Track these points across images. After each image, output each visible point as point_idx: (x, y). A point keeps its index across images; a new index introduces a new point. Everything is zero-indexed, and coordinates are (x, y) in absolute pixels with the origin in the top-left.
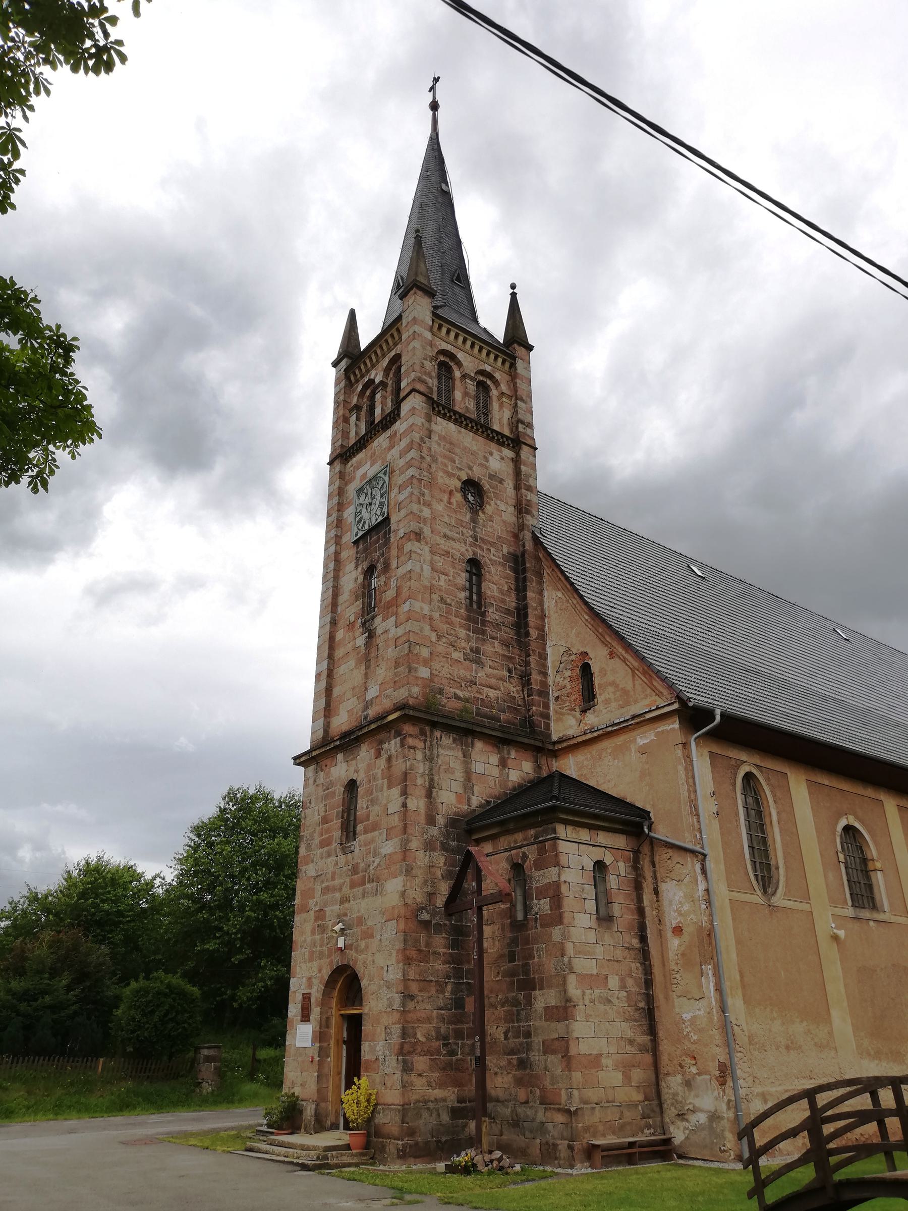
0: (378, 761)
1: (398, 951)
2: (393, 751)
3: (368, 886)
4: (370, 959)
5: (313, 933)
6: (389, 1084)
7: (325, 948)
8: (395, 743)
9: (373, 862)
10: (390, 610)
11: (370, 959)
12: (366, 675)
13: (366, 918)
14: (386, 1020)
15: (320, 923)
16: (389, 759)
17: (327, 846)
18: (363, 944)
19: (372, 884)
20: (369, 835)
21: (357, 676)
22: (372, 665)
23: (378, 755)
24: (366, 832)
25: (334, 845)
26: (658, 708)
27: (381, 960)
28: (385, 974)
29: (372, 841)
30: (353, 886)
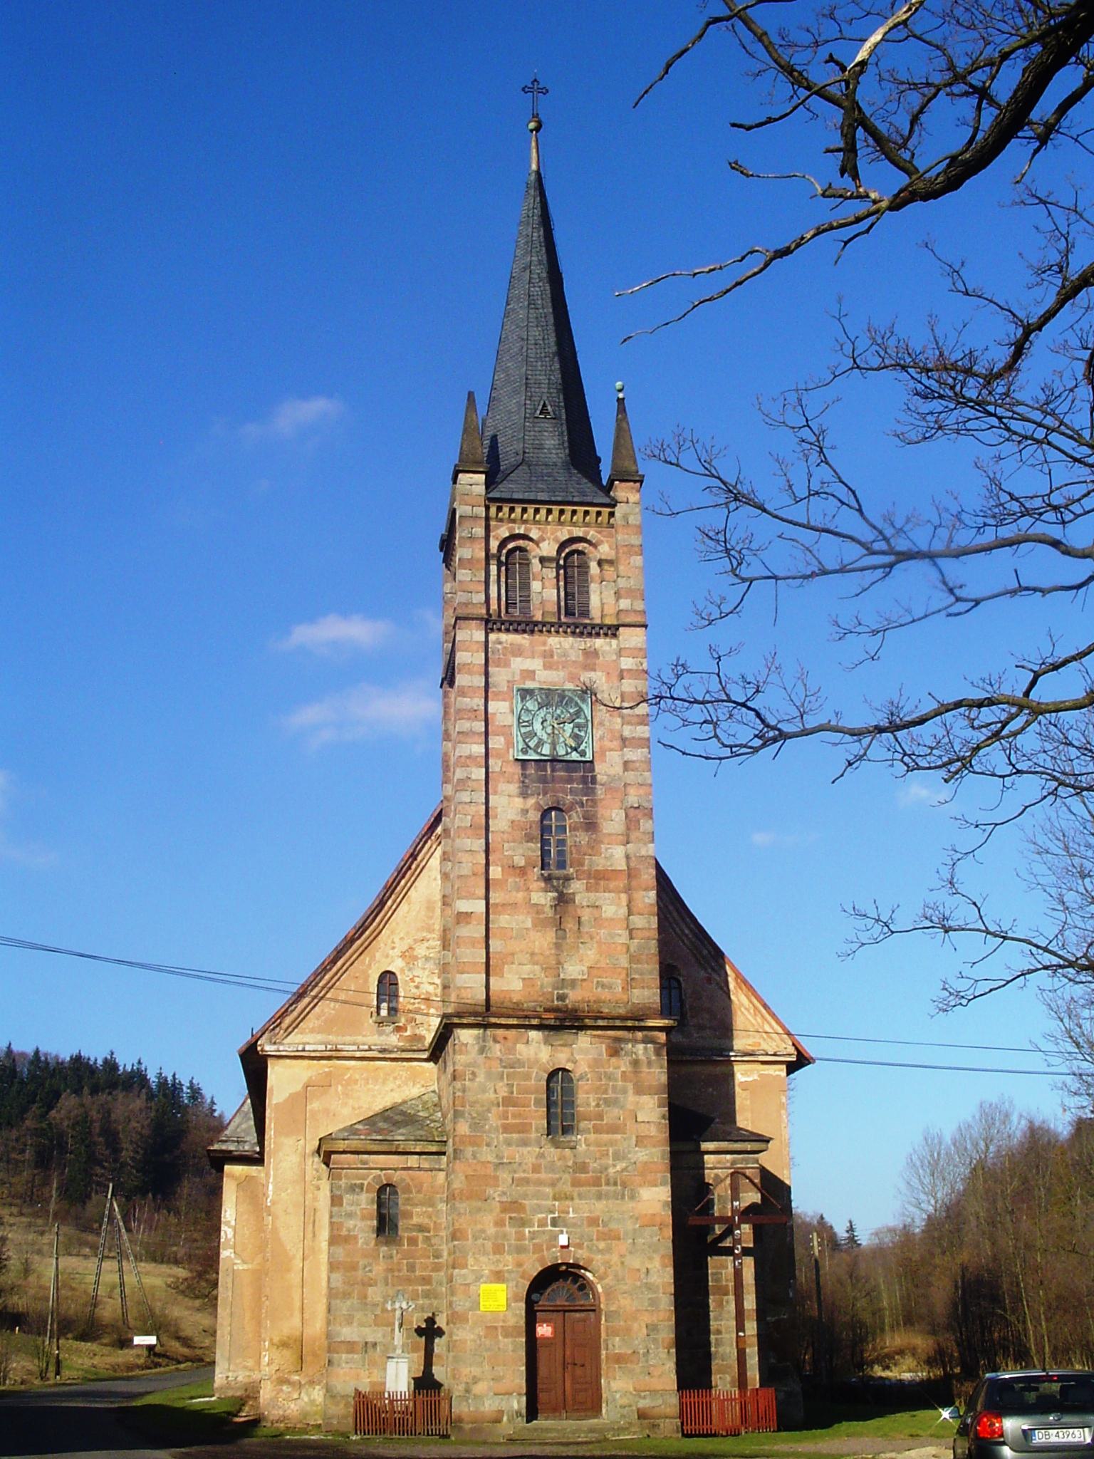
0: (613, 1060)
1: (663, 1257)
2: (642, 1057)
3: (604, 1188)
4: (615, 1258)
5: (499, 1223)
6: (656, 1373)
7: (527, 1242)
8: (646, 1049)
9: (614, 1166)
10: (602, 883)
11: (615, 1258)
12: (558, 946)
13: (605, 1219)
14: (646, 1318)
15: (513, 1215)
16: (636, 1063)
17: (519, 1132)
18: (602, 1245)
19: (612, 1188)
20: (605, 1137)
21: (544, 940)
22: (570, 939)
23: (615, 1052)
24: (597, 1130)
25: (533, 1135)
26: (775, 1055)
27: (635, 1262)
28: (643, 1276)
29: (612, 1143)
30: (576, 1183)
